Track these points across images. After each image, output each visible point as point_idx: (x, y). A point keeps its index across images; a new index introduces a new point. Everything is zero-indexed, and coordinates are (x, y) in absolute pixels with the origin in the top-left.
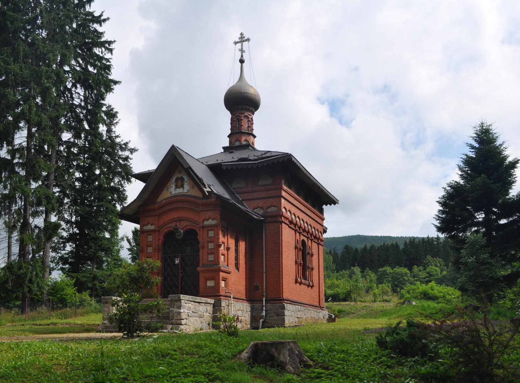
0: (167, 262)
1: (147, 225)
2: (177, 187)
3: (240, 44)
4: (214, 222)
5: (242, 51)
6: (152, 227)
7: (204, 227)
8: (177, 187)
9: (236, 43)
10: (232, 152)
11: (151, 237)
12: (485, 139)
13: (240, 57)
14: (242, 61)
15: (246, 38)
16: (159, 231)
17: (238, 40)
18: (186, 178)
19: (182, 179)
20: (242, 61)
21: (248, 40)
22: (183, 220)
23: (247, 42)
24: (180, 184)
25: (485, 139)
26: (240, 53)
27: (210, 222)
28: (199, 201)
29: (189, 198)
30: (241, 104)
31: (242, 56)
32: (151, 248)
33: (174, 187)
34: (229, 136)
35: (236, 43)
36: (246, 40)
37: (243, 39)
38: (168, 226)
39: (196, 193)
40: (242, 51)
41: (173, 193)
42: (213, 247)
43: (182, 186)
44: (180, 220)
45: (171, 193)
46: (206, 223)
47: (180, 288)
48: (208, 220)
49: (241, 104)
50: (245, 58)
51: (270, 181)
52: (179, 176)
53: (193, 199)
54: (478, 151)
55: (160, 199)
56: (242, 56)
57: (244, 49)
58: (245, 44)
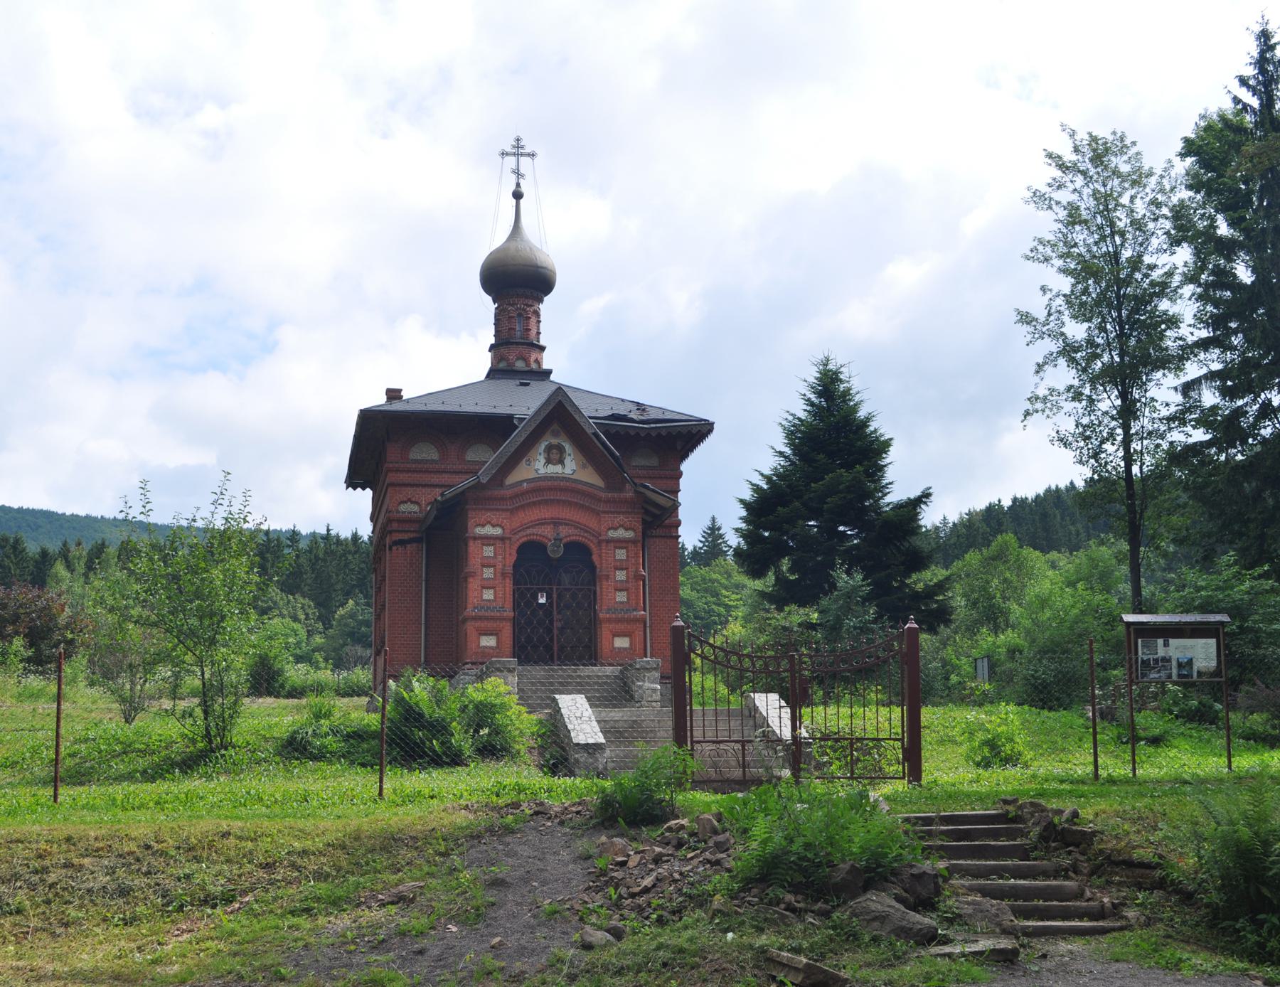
0: (523, 599)
1: (483, 526)
2: (549, 461)
3: (513, 159)
4: (630, 534)
5: (518, 173)
6: (498, 531)
7: (608, 541)
8: (549, 461)
9: (504, 154)
10: (527, 384)
11: (491, 548)
12: (830, 390)
13: (513, 187)
14: (518, 195)
15: (527, 150)
16: (510, 539)
17: (509, 150)
18: (568, 447)
19: (561, 450)
20: (518, 195)
21: (532, 155)
22: (561, 524)
23: (528, 159)
24: (555, 455)
25: (830, 390)
26: (514, 177)
27: (621, 533)
28: (603, 495)
29: (580, 487)
30: (516, 285)
31: (518, 185)
32: (492, 570)
33: (543, 461)
34: (492, 348)
35: (504, 154)
36: (529, 155)
37: (518, 150)
38: (528, 532)
39: (590, 477)
40: (518, 173)
41: (542, 471)
42: (624, 578)
43: (561, 462)
44: (556, 523)
45: (537, 470)
46: (612, 534)
47: (555, 648)
48: (616, 529)
49: (516, 285)
50: (524, 189)
51: (654, 461)
52: (555, 441)
53: (590, 490)
54: (816, 410)
55: (512, 479)
56: (518, 185)
57: (522, 171)
58: (522, 159)
